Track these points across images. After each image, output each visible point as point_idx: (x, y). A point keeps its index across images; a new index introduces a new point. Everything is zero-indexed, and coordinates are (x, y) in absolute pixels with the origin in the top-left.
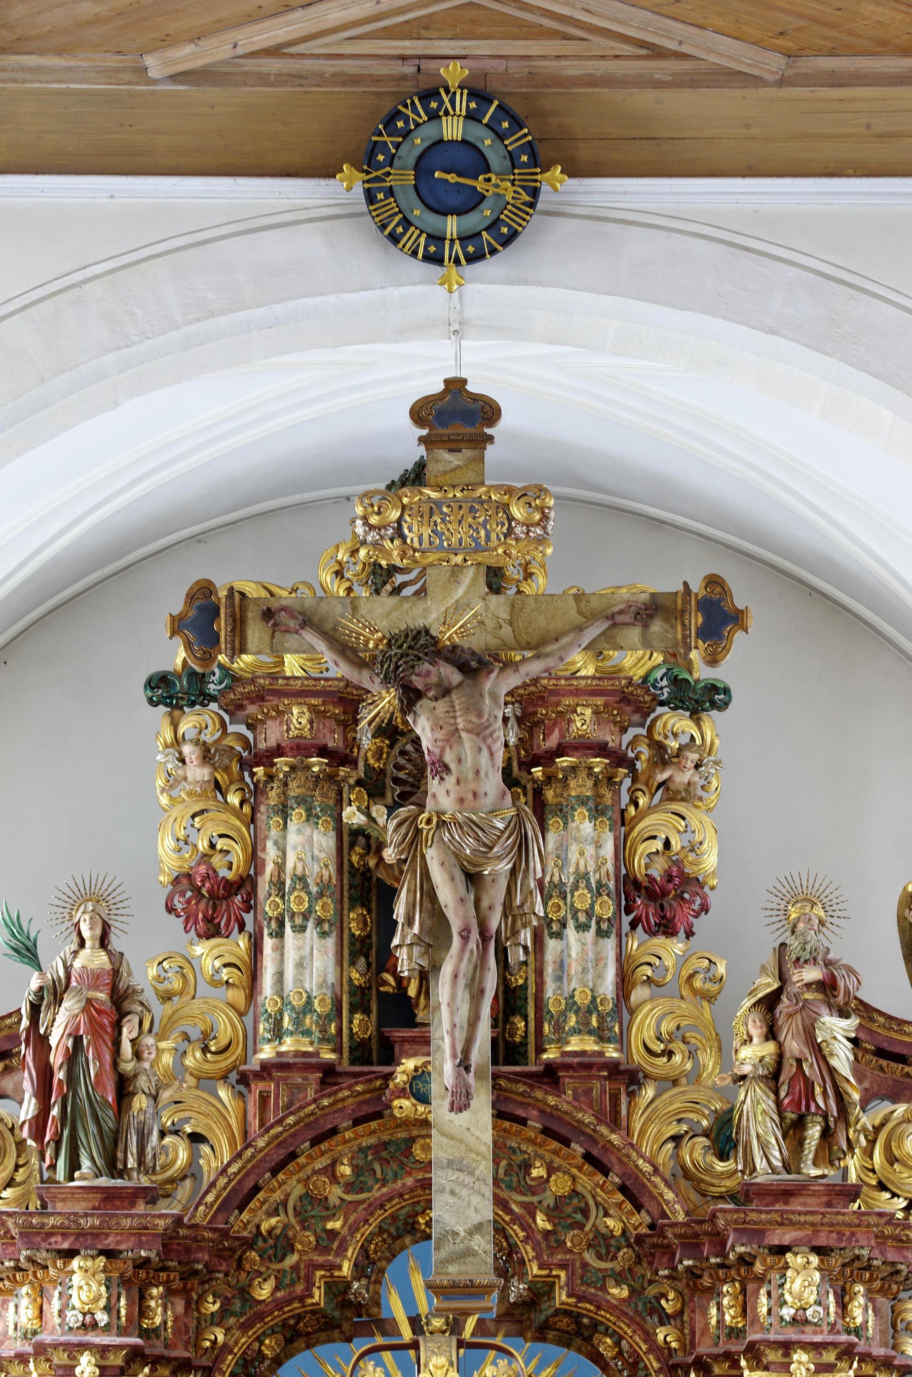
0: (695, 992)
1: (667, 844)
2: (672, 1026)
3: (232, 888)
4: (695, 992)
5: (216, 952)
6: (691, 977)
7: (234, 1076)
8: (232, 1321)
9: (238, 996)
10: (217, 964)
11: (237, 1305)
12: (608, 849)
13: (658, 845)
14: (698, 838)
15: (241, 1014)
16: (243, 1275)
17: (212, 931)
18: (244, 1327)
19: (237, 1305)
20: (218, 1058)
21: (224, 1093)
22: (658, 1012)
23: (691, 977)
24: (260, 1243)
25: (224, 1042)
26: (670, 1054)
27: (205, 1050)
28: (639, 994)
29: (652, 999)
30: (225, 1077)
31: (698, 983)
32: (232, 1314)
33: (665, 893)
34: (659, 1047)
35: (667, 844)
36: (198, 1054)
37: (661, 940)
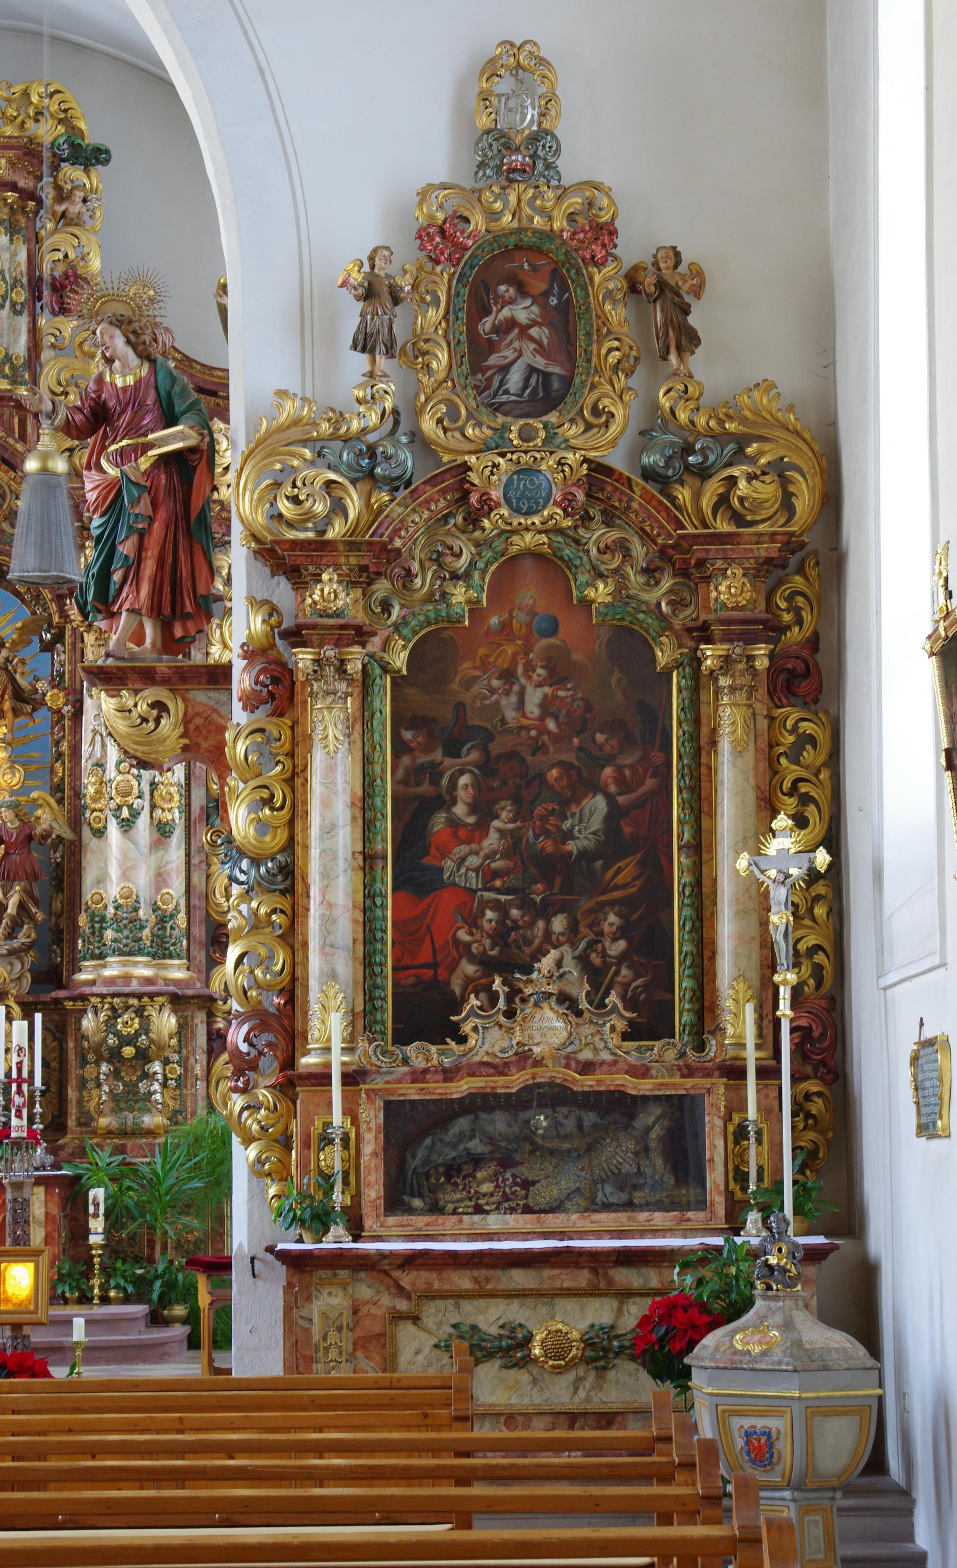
0: (84, 353)
1: (66, 256)
2: (68, 375)
4: (84, 353)
6: (81, 344)
12: (23, 256)
13: (60, 256)
14: (86, 250)
22: (58, 366)
23: (81, 344)
26: (66, 394)
28: (46, 355)
29: (55, 358)
31: (86, 348)
33: (63, 287)
34: (59, 390)
35: (66, 256)
37: (61, 318)
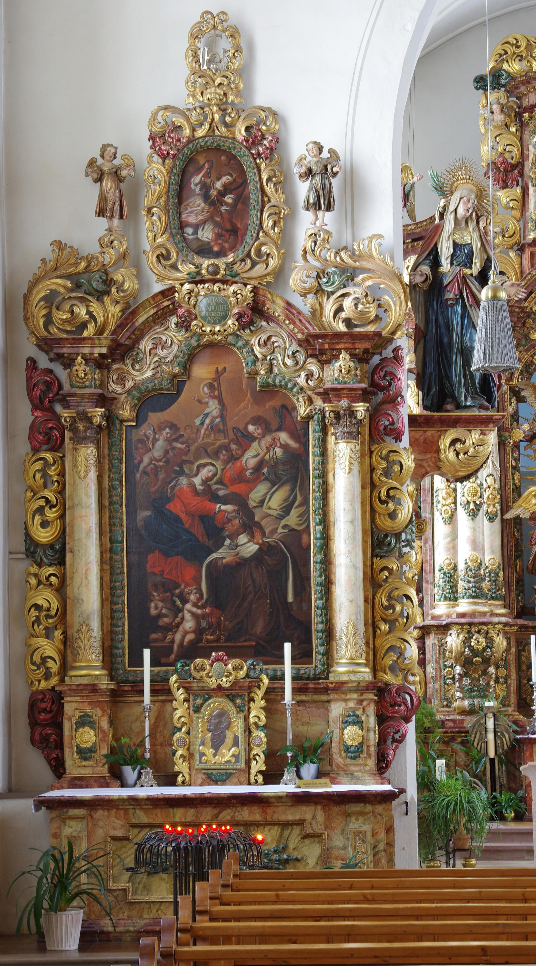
3: (514, 167)
5: (507, 194)
7: (516, 248)
8: (521, 348)
9: (517, 213)
10: (508, 200)
11: (523, 342)
15: (518, 221)
16: (526, 329)
17: (505, 186)
18: (527, 351)
19: (523, 342)
20: (509, 239)
21: (511, 254)
24: (532, 316)
25: (511, 233)
27: (504, 236)
30: (512, 248)
32: (521, 346)
36: (501, 238)
